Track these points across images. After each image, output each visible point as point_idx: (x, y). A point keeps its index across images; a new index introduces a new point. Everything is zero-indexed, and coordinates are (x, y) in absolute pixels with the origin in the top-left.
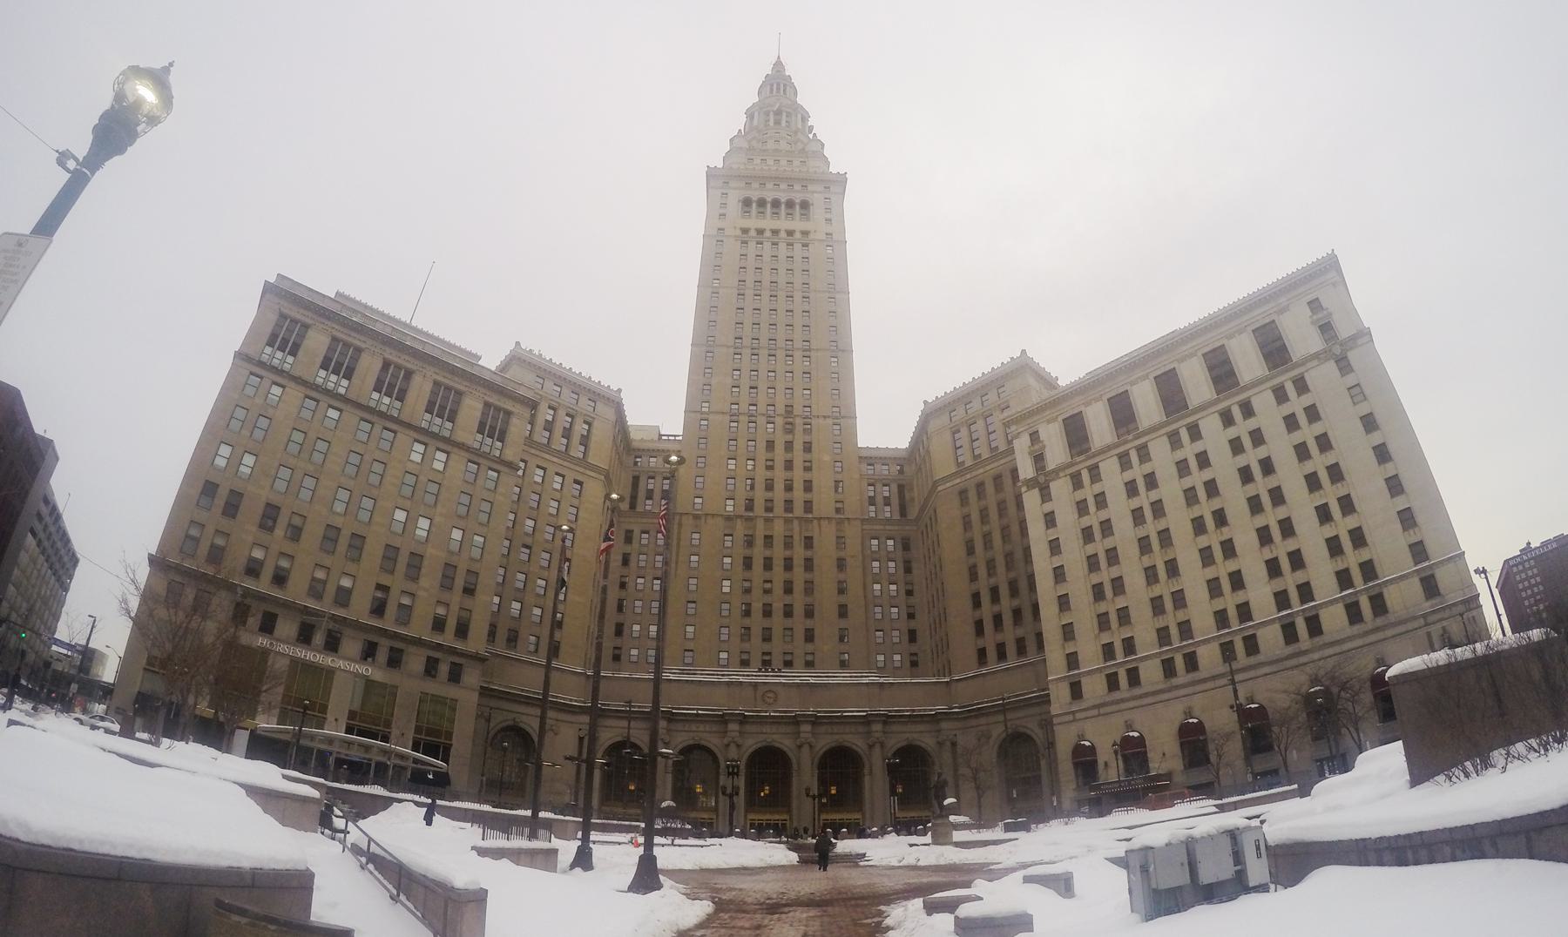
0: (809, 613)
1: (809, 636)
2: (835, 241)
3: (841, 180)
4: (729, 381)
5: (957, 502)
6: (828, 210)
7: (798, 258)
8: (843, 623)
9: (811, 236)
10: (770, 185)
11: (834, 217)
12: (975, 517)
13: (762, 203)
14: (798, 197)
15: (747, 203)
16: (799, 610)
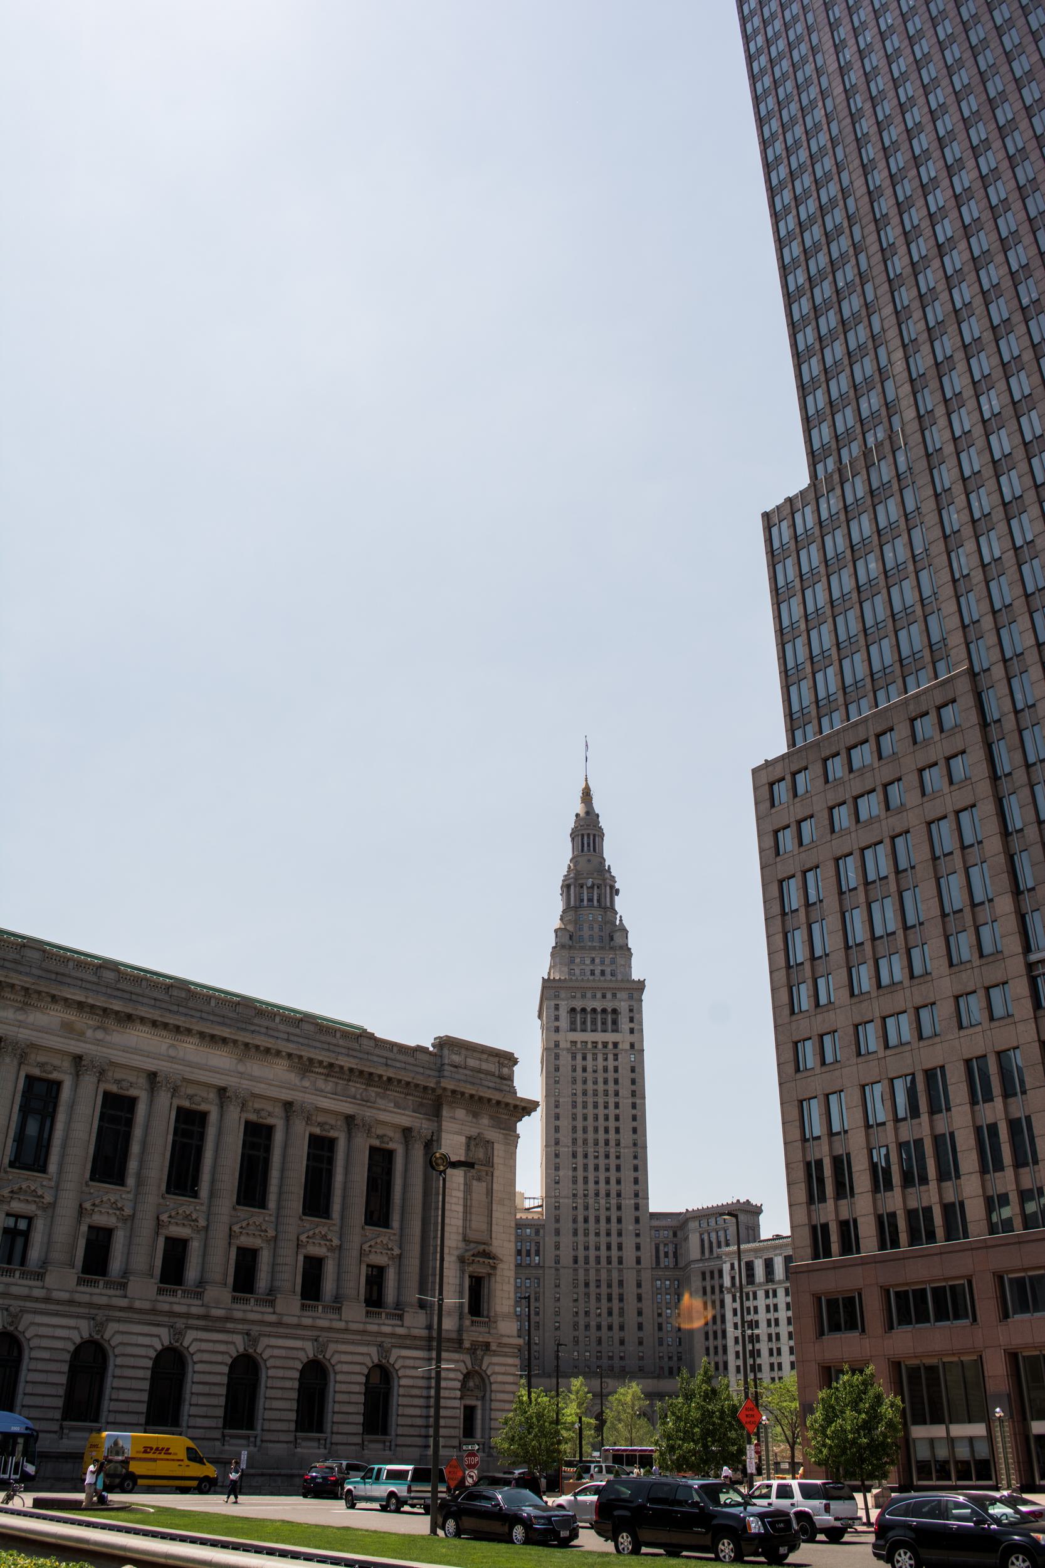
0: (622, 1328)
1: (622, 1342)
2: (636, 1049)
3: (640, 986)
4: (570, 1173)
5: (700, 1277)
6: (631, 1020)
7: (611, 1068)
8: (641, 1334)
9: (620, 1046)
10: (589, 995)
11: (636, 1030)
12: (709, 1289)
13: (584, 1010)
14: (609, 1006)
15: (573, 1010)
16: (616, 1327)
